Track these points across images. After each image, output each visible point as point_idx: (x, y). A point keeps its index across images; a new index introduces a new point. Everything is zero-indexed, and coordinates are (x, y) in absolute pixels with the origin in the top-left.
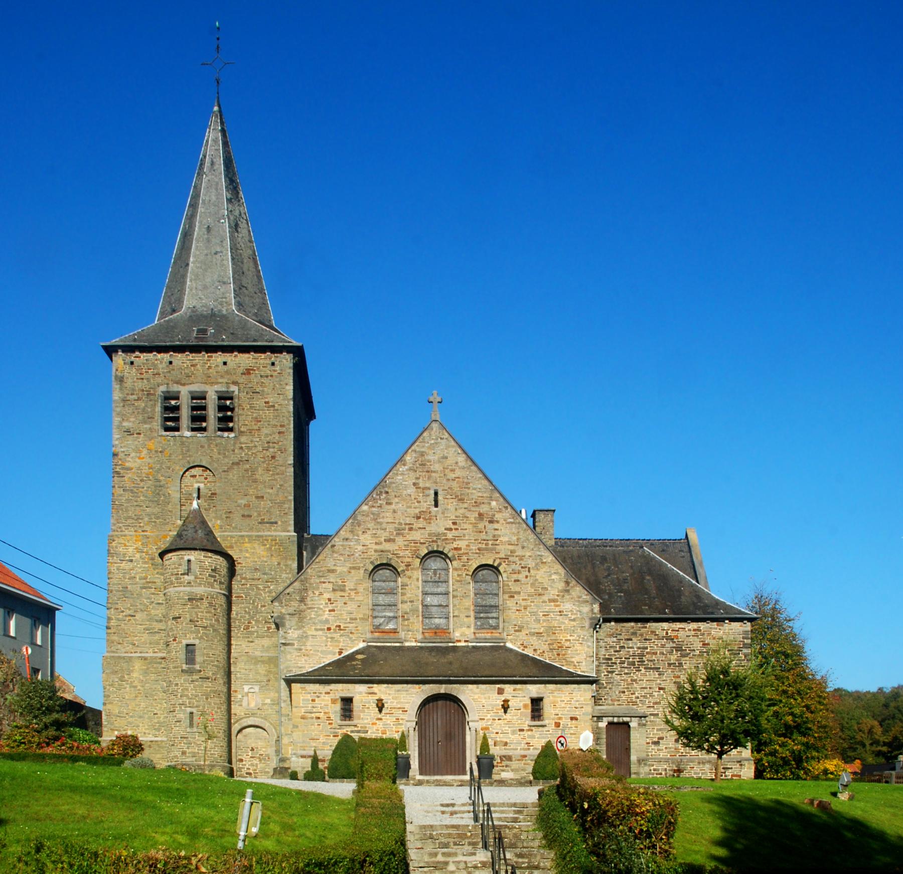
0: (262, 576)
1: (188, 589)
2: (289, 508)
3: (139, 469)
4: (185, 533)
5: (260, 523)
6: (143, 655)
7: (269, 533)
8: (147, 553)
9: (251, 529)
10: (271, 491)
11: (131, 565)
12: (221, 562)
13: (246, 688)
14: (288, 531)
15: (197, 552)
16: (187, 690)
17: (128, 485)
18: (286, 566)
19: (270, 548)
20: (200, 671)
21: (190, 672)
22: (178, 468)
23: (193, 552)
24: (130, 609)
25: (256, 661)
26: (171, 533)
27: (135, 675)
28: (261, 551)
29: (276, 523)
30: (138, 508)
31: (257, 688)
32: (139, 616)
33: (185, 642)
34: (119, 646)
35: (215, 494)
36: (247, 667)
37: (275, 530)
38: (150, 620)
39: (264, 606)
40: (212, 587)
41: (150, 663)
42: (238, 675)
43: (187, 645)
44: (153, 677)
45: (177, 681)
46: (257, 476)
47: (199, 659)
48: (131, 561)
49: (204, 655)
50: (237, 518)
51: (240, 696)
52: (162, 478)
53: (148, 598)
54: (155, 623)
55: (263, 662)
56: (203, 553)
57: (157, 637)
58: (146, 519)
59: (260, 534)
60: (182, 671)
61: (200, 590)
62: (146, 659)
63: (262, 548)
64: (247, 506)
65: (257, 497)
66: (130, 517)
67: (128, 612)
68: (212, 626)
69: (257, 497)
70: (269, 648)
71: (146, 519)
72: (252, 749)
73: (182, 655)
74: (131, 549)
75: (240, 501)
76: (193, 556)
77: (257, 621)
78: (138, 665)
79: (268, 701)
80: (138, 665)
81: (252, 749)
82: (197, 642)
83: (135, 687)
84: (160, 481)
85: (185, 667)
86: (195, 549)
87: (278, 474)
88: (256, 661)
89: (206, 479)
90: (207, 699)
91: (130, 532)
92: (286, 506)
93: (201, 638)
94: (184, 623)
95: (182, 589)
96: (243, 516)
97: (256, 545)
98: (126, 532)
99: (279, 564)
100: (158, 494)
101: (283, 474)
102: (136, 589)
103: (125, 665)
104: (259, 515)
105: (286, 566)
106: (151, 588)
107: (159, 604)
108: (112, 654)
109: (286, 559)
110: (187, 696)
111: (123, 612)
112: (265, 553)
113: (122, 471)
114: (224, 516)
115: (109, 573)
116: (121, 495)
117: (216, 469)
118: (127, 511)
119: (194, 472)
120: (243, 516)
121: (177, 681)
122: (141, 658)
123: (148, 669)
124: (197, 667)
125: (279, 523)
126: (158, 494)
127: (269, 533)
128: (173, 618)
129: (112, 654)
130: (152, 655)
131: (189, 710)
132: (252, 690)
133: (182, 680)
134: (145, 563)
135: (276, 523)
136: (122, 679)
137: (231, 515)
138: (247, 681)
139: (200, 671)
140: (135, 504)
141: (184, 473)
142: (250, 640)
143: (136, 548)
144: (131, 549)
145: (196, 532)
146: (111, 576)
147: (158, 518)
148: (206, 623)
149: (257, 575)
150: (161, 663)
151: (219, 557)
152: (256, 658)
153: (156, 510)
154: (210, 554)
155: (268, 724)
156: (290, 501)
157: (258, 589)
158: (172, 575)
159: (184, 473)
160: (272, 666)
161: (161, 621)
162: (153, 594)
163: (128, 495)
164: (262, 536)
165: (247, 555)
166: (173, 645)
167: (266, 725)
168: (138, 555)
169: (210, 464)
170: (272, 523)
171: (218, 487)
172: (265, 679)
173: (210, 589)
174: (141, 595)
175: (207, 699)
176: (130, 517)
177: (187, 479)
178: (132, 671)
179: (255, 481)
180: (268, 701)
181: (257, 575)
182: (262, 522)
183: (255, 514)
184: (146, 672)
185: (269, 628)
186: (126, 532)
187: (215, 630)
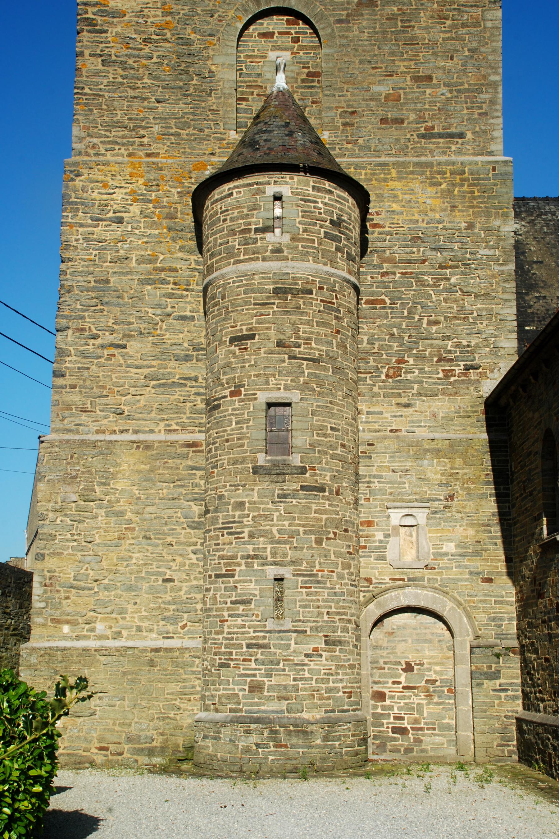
0: (430, 254)
1: (274, 266)
2: (492, 102)
3: (140, 13)
4: (265, 136)
5: (423, 136)
6: (141, 437)
7: (445, 158)
8: (157, 203)
9: (403, 150)
10: (449, 64)
11: (117, 231)
12: (348, 205)
13: (396, 517)
14: (491, 153)
15: (298, 178)
16: (268, 518)
17: (115, 50)
18: (488, 230)
19: (450, 192)
20: (303, 471)
21: (277, 471)
22: (231, 13)
23: (287, 176)
24: (112, 332)
25: (419, 450)
26: (214, 159)
27: (120, 484)
28: (427, 196)
29: (461, 135)
30: (136, 104)
31: (421, 516)
32: (134, 347)
33: (263, 397)
34: (84, 417)
35: (317, 74)
36: (396, 465)
37: (459, 152)
38: (163, 355)
39: (437, 323)
40: (333, 262)
41: (158, 456)
42: (376, 485)
43: (270, 405)
44: (166, 490)
45: (241, 495)
46: (417, 31)
47: (300, 440)
48: (120, 221)
49: (312, 428)
50: (368, 125)
51: (379, 536)
52: (193, 36)
53: (159, 306)
54: (173, 363)
55: (437, 453)
56: (312, 180)
57: (178, 395)
58: (156, 128)
59: (423, 159)
60: (256, 470)
61: (304, 269)
62: (148, 446)
63: (431, 190)
64: (393, 98)
65: (417, 79)
66: (118, 125)
67: (109, 338)
68: (332, 359)
69: (417, 79)
70: (448, 419)
71: (156, 128)
72: (409, 668)
73: (256, 431)
74: (119, 195)
75: (376, 88)
76: (288, 185)
77: (420, 357)
78: (128, 462)
79: (450, 547)
80: (128, 462)
81: (409, 668)
82: (294, 396)
83: (121, 514)
84: (188, 43)
85: (262, 459)
86: (293, 168)
87: (464, 25)
88: (419, 450)
89: (296, 40)
90: (319, 542)
91: (118, 157)
92: (485, 96)
93: (305, 388)
94: (262, 349)
95: (259, 265)
96: (383, 121)
97: (416, 186)
98: (109, 157)
99: (470, 226)
100: (186, 72)
101: (476, 24)
102: (130, 284)
103: (96, 463)
104: (421, 119)
105: (488, 230)
106: (165, 282)
107: (183, 318)
108: (66, 437)
109: (488, 215)
110: (267, 534)
111: (95, 337)
112: (437, 203)
113: (99, 20)
114: (339, 122)
115: (68, 247)
116: (97, 74)
117: (322, 17)
118: (111, 109)
119: (267, 24)
120: (383, 121)
121: (241, 495)
122: (138, 444)
123: (152, 470)
124: (296, 460)
125: (469, 135)
126: (186, 72)
127: (445, 158)
128: (233, 340)
129: (66, 437)
130: (162, 436)
131: (272, 571)
132: (409, 521)
133: (257, 492)
134: (154, 225)
135: (461, 135)
136: (87, 497)
137: (356, 120)
138: (398, 500)
139: (303, 471)
140: (131, 93)
141: (246, 27)
142: (404, 400)
143: (133, 192)
144: (119, 195)
145: (291, 134)
146: (66, 255)
147: (185, 126)
148: (317, 349)
149: (418, 253)
150: (185, 457)
151: (346, 195)
152: (418, 443)
153: (181, 107)
154: (327, 185)
155: (450, 605)
156: (494, 85)
157: (422, 284)
158: (232, 232)
159: (246, 27)
160: (459, 462)
161: (187, 358)
162: (170, 296)
163: (113, 74)
164: (431, 165)
165: (395, 207)
166: (230, 406)
167: (446, 608)
168: (135, 209)
169: (307, 5)
170: (452, 136)
171: (324, 58)
172: (442, 494)
173: (328, 268)
174: (141, 299)
175: (319, 542)
176: (118, 125)
177: (253, 41)
178: (114, 476)
179: (412, 42)
180: (450, 547)
181: (418, 253)
182: (428, 135)
183: (412, 117)
184: (147, 479)
185: (448, 374)
186: (109, 157)
187: (337, 370)
